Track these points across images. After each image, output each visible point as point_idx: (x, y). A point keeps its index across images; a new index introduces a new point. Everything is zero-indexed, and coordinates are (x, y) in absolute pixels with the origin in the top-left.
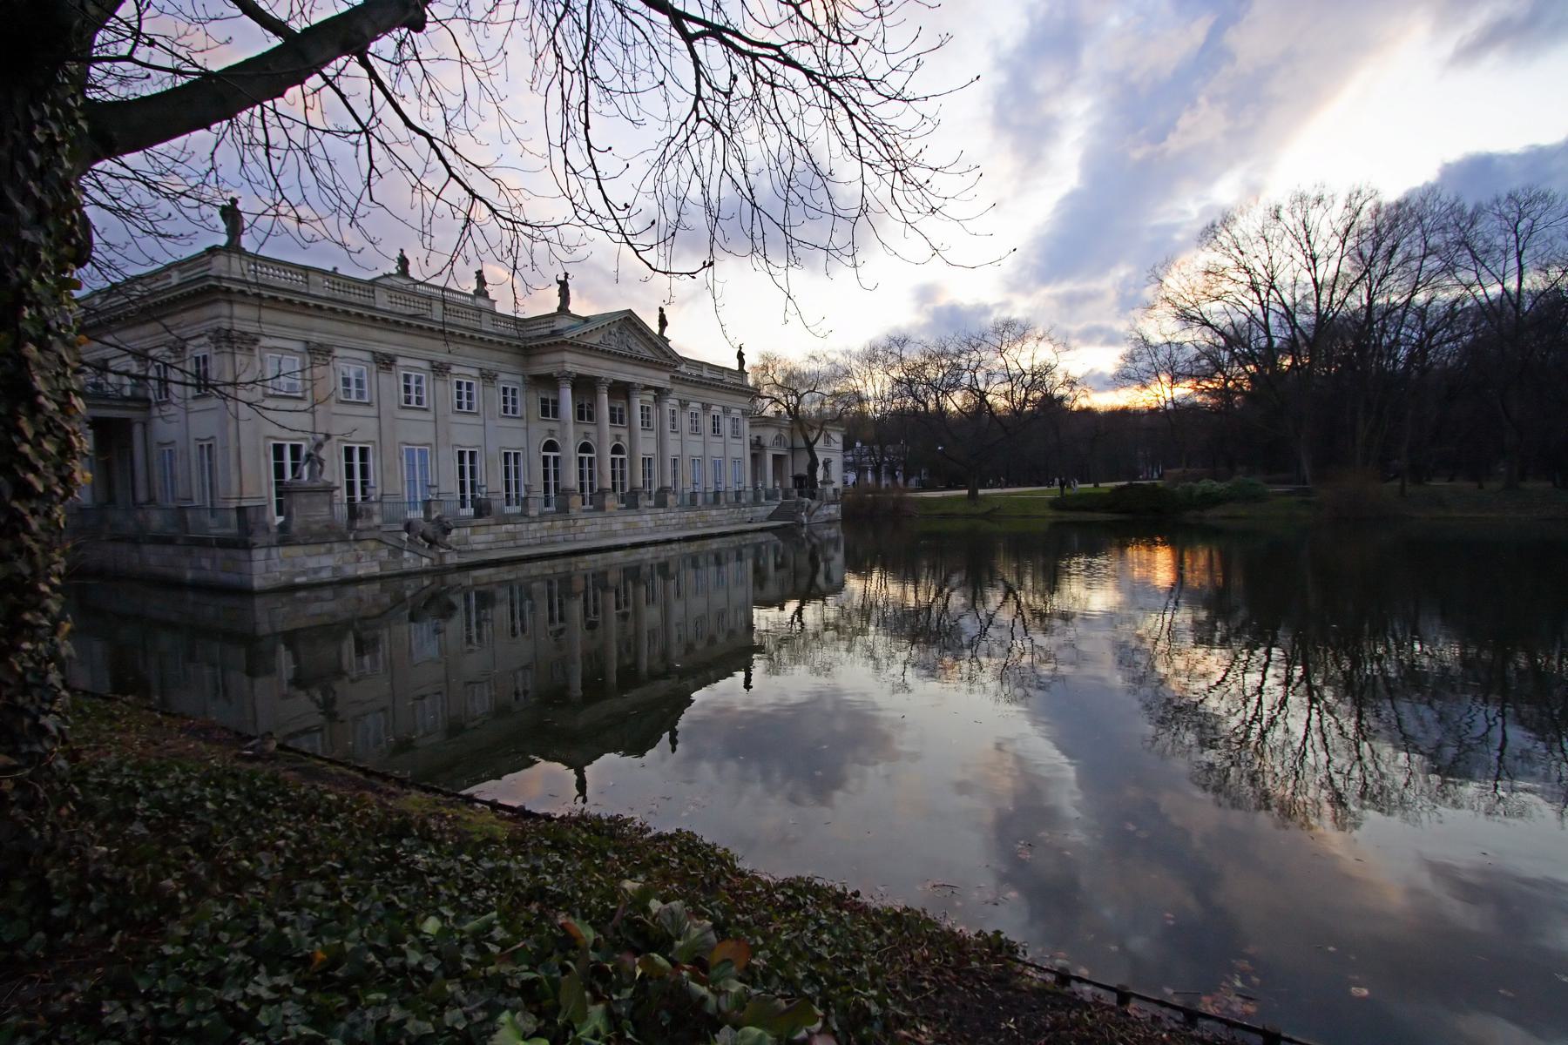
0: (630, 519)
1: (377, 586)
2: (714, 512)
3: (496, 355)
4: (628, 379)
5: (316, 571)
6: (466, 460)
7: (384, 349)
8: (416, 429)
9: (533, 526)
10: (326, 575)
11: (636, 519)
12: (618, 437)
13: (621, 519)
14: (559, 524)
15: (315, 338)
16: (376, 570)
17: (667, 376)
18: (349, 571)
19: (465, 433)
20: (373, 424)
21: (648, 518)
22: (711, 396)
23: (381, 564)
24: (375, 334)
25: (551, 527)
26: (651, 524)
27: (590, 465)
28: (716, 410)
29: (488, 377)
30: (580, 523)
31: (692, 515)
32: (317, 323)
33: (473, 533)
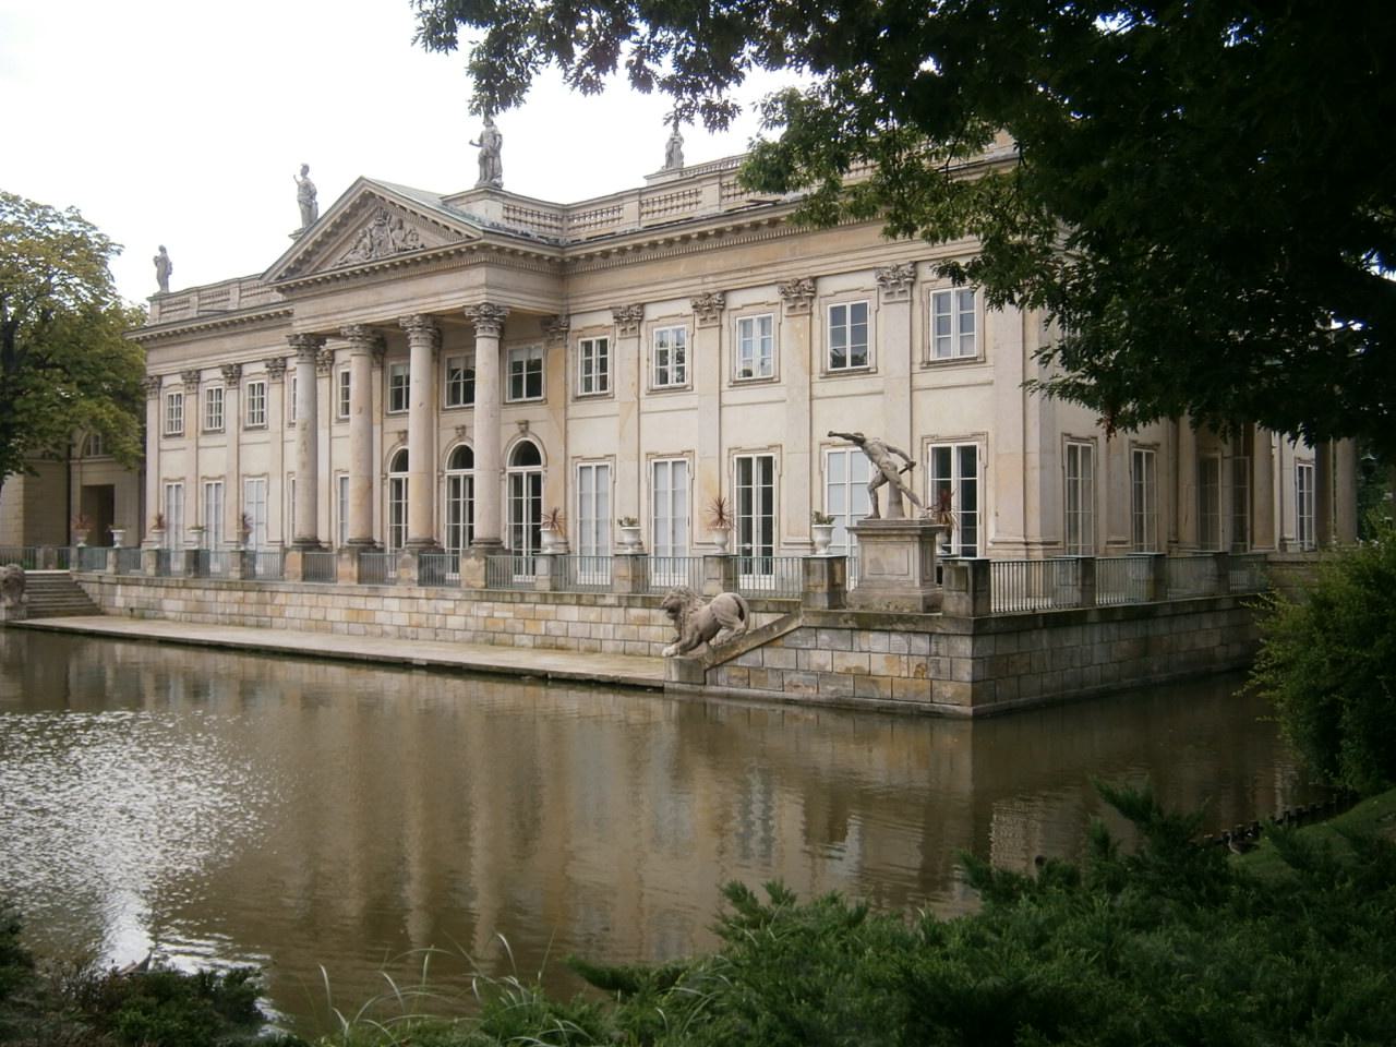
0: (359, 603)
2: (571, 613)
7: (232, 359)
9: (223, 596)
11: (373, 604)
12: (525, 426)
13: (342, 601)
14: (253, 596)
15: (191, 364)
21: (394, 604)
24: (228, 343)
25: (242, 602)
26: (402, 620)
27: (537, 490)
28: (841, 289)
30: (280, 599)
31: (503, 612)
32: (194, 348)
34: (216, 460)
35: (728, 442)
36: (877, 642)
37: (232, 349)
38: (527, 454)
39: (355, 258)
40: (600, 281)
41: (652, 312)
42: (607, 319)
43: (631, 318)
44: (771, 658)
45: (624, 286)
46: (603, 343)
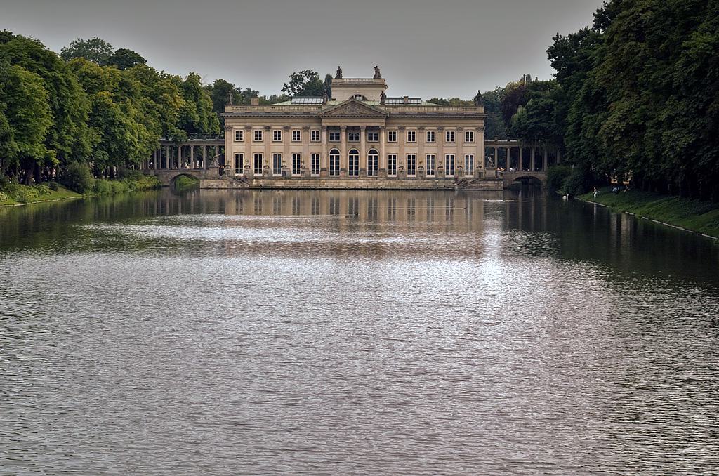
1: (226, 191)
3: (309, 121)
4: (357, 125)
5: (212, 186)
6: (296, 159)
8: (277, 148)
10: (215, 187)
15: (247, 124)
16: (226, 187)
17: (384, 121)
18: (220, 186)
19: (296, 148)
20: (263, 147)
22: (443, 123)
23: (228, 185)
24: (265, 120)
29: (306, 129)
32: (248, 120)
33: (277, 181)
34: (258, 148)
35: (425, 152)
36: (490, 182)
37: (268, 122)
38: (373, 152)
39: (347, 113)
40: (394, 121)
41: (407, 128)
42: (396, 128)
43: (402, 129)
44: (473, 185)
45: (402, 123)
46: (394, 133)
